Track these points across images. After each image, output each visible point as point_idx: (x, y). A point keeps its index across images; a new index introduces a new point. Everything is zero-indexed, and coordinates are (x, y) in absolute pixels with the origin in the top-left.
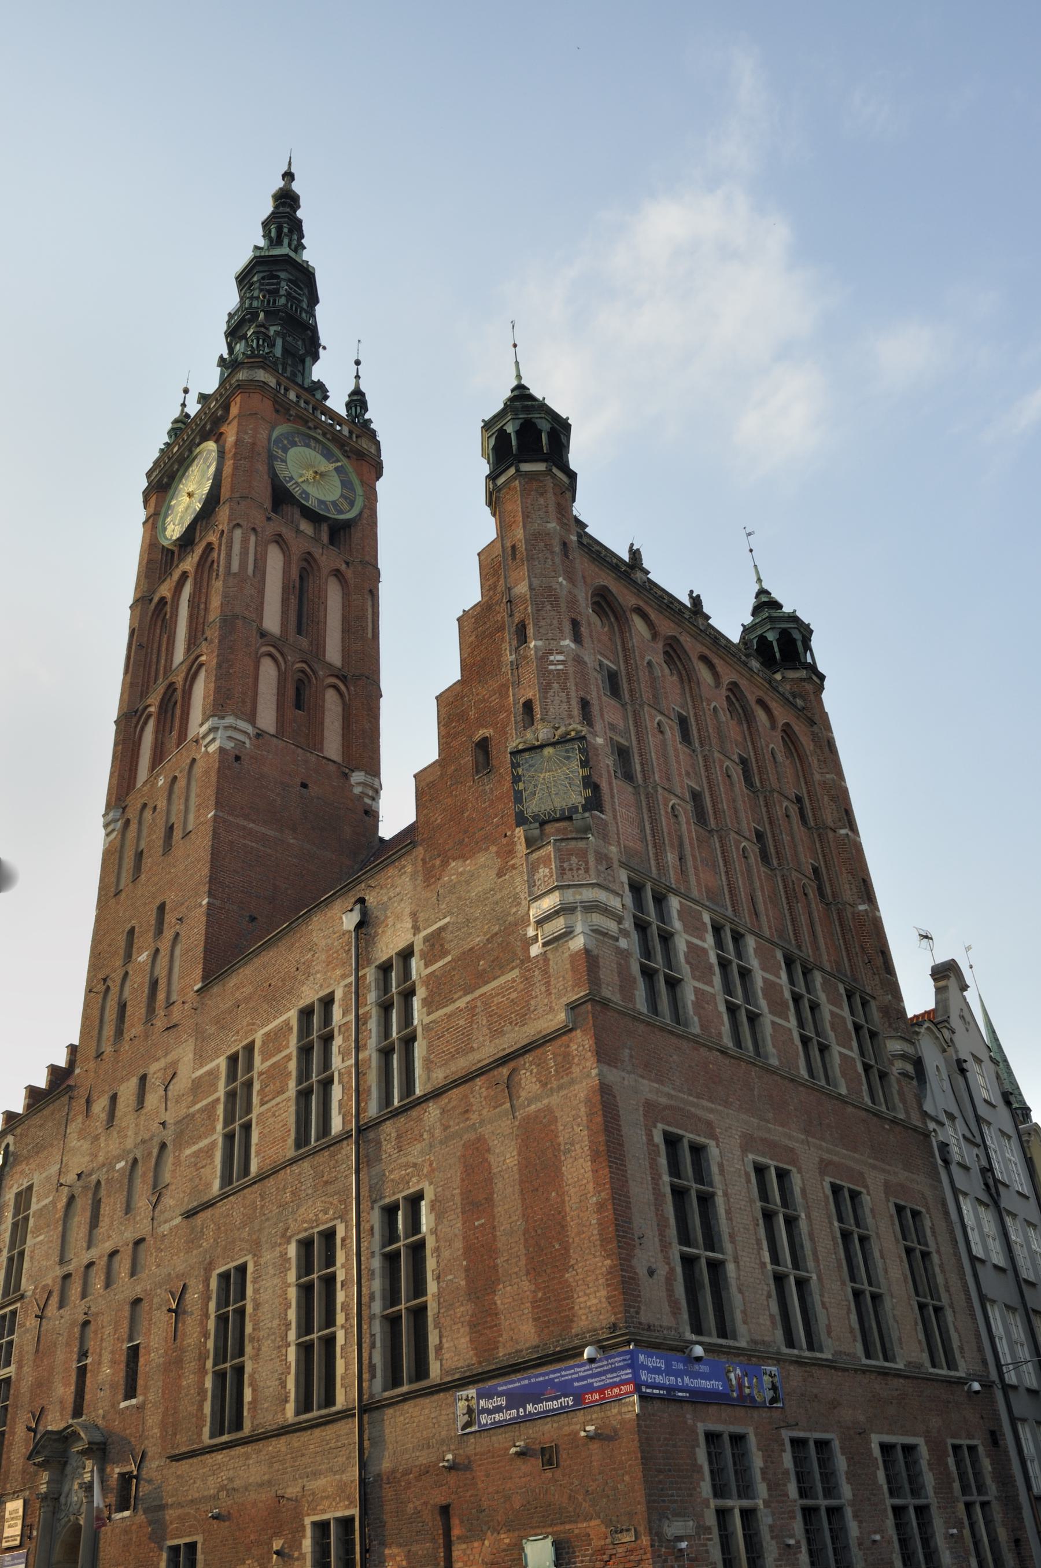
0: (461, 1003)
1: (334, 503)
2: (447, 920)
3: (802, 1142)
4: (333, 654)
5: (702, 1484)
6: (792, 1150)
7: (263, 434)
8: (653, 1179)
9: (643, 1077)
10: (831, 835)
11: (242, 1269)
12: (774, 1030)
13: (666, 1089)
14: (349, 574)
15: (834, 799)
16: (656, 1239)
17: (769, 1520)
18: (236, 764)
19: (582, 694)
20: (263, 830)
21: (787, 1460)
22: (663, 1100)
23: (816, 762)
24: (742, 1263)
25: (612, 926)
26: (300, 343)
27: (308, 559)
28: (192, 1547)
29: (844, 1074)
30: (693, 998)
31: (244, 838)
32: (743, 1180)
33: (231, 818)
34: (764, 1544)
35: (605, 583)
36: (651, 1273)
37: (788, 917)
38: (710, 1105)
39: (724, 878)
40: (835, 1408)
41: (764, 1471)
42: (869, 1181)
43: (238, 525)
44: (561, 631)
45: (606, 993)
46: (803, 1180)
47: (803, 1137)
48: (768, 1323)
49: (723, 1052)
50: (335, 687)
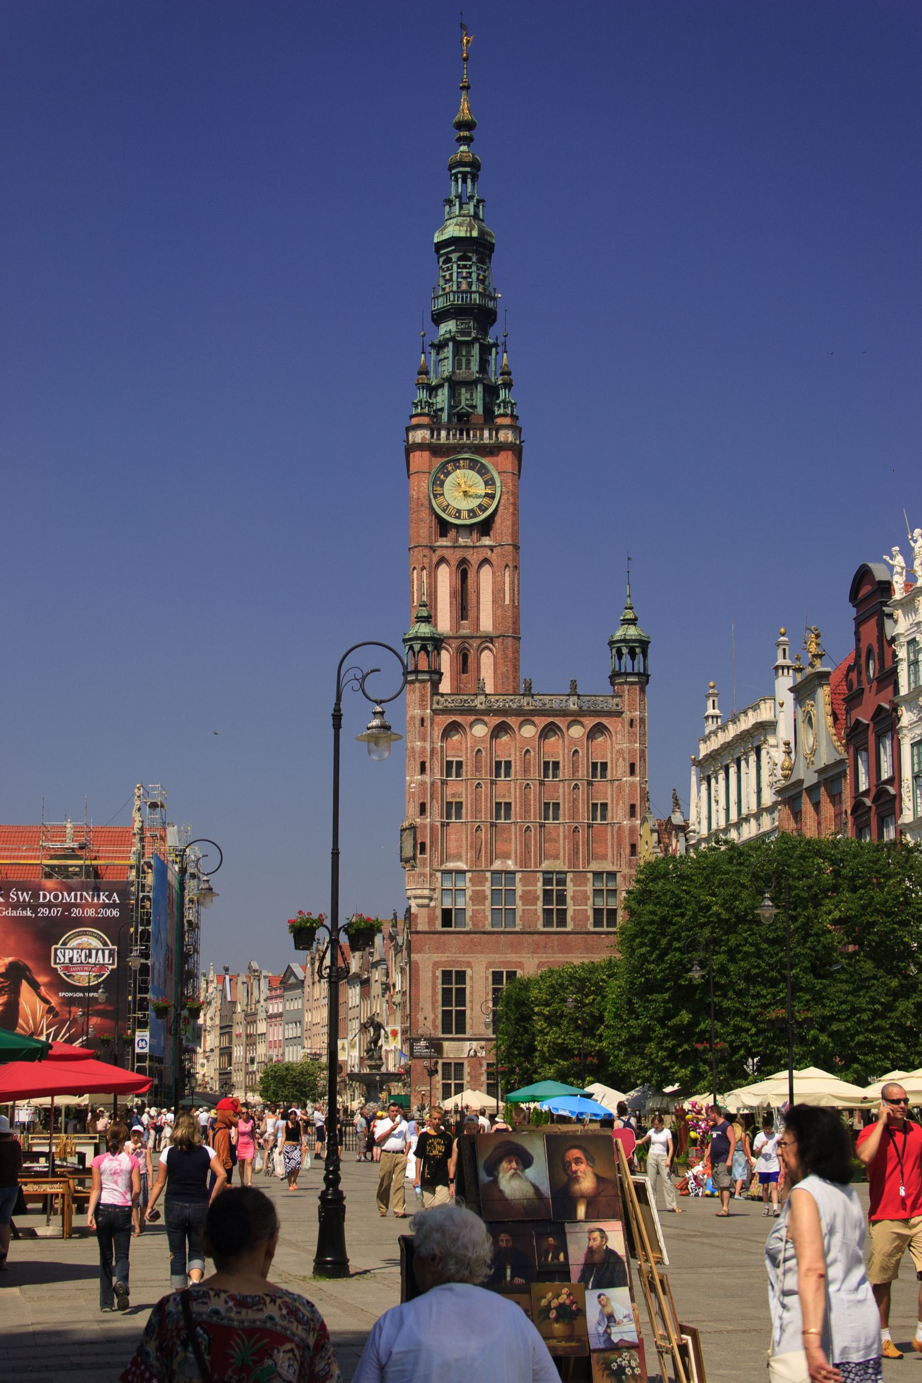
1: (480, 506)
4: (486, 624)
7: (425, 485)
10: (616, 783)
14: (493, 557)
15: (624, 760)
19: (421, 801)
22: (445, 959)
25: (426, 901)
26: (471, 324)
27: (464, 562)
29: (573, 919)
35: (454, 718)
36: (425, 1018)
37: (562, 845)
39: (513, 845)
43: (414, 568)
45: (420, 928)
49: (484, 933)
50: (487, 648)
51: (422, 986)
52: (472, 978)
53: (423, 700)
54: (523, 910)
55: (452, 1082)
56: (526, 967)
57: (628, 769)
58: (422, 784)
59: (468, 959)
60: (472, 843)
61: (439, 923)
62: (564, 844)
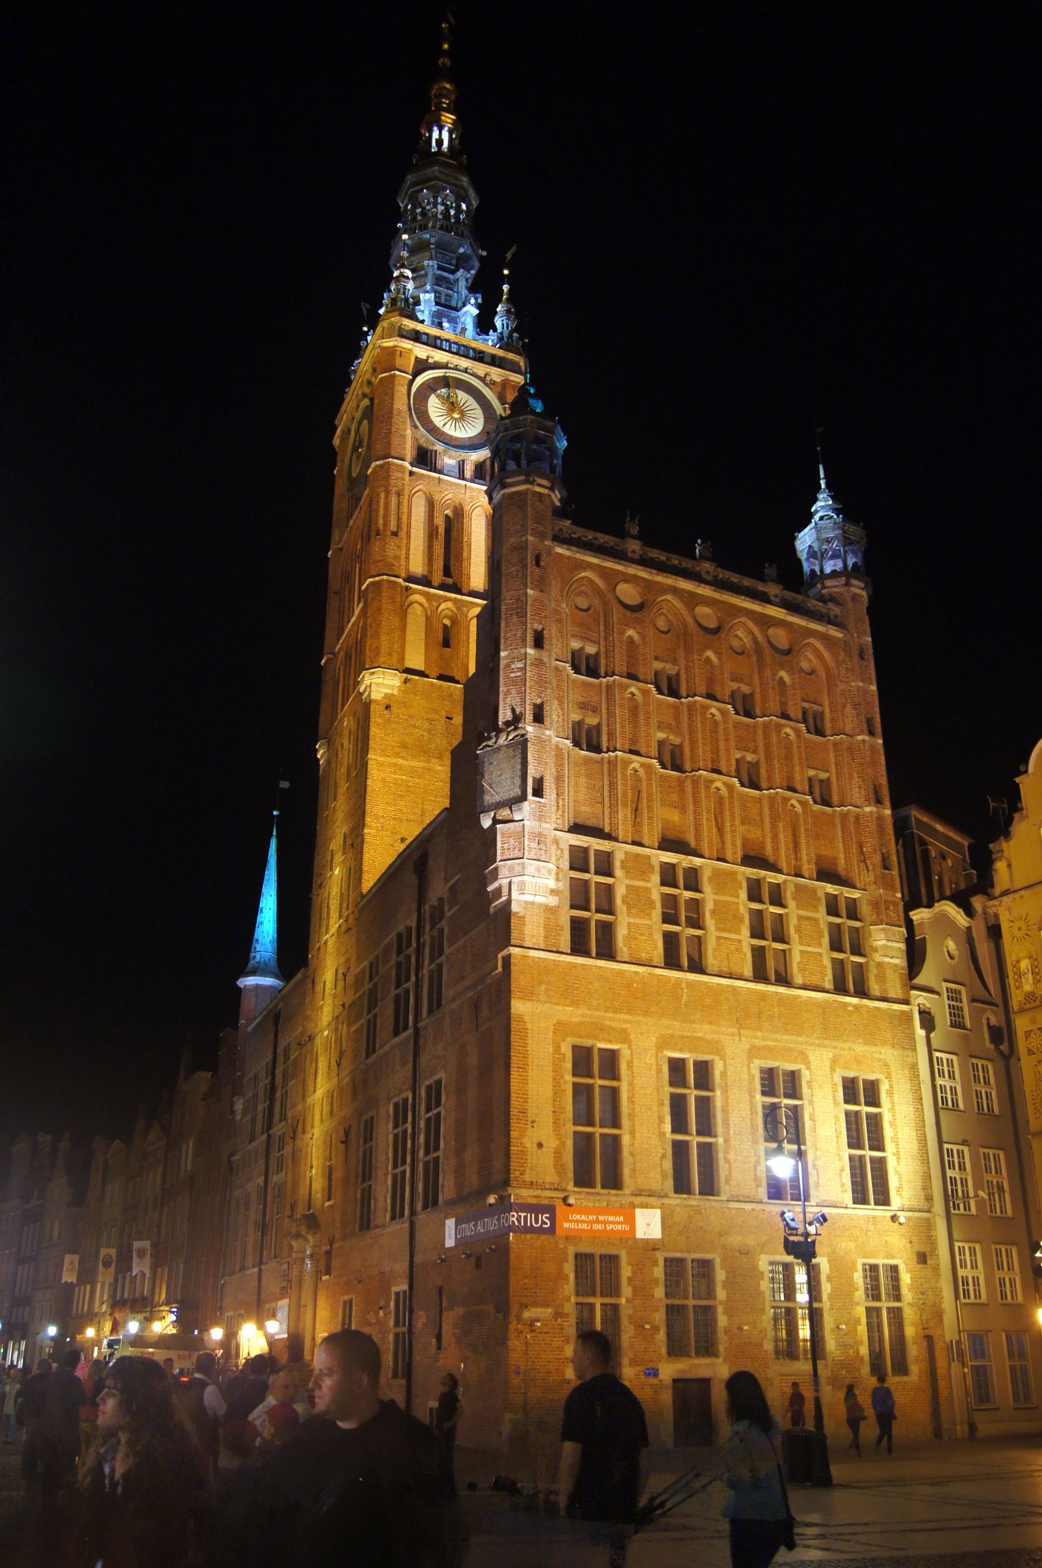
0: (461, 943)
2: (458, 876)
3: (733, 1035)
5: (565, 1286)
6: (716, 1042)
8: (554, 1079)
9: (557, 1004)
11: (372, 1118)
12: (719, 945)
13: (580, 1012)
15: (855, 706)
16: (551, 1124)
17: (631, 1311)
18: (385, 712)
20: (412, 763)
21: (659, 1272)
22: (576, 1020)
23: (843, 672)
24: (638, 1135)
28: (351, 1301)
30: (625, 932)
31: (395, 773)
32: (654, 1073)
33: (382, 759)
34: (622, 1327)
36: (540, 1145)
38: (627, 1017)
39: (691, 817)
40: (721, 1236)
41: (630, 1280)
42: (812, 1058)
44: (524, 640)
46: (725, 1066)
47: (736, 1031)
48: (659, 1176)
51: (533, 1073)
52: (630, 1064)
53: (539, 523)
54: (718, 938)
55: (598, 1302)
56: (729, 1051)
57: (865, 725)
58: (539, 663)
59: (624, 1026)
60: (624, 795)
61: (565, 940)
62: (774, 827)
